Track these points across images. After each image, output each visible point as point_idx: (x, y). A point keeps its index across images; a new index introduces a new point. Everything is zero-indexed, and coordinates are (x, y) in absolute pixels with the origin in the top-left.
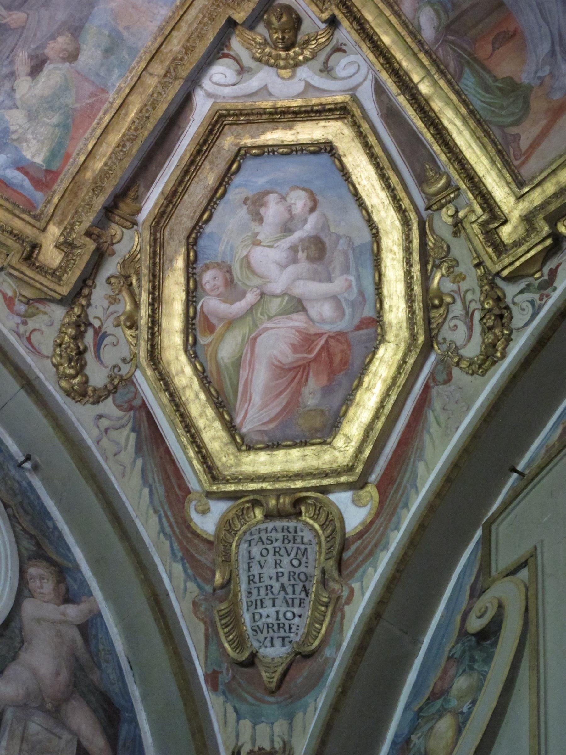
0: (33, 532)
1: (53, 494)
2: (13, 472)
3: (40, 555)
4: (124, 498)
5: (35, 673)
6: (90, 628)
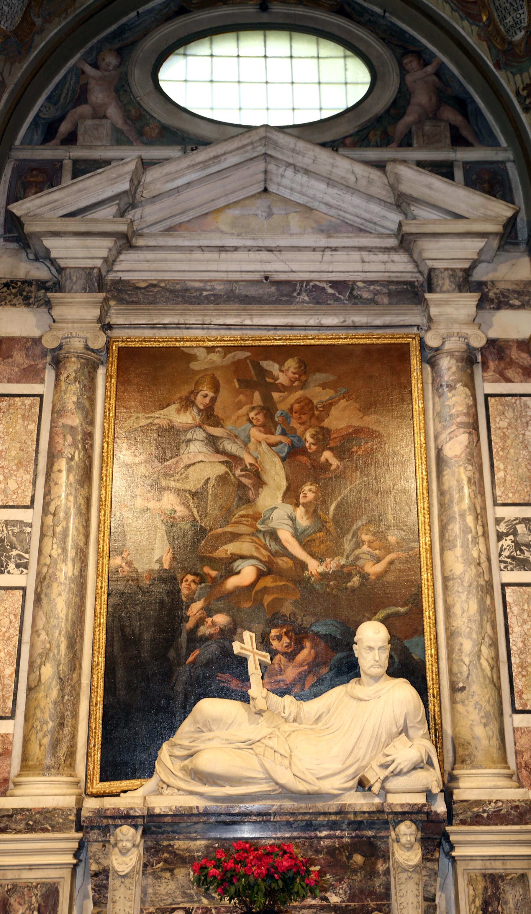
0: (400, 43)
1: (404, 21)
2: (382, 21)
3: (407, 52)
4: (430, 5)
5: (420, 105)
6: (440, 72)
